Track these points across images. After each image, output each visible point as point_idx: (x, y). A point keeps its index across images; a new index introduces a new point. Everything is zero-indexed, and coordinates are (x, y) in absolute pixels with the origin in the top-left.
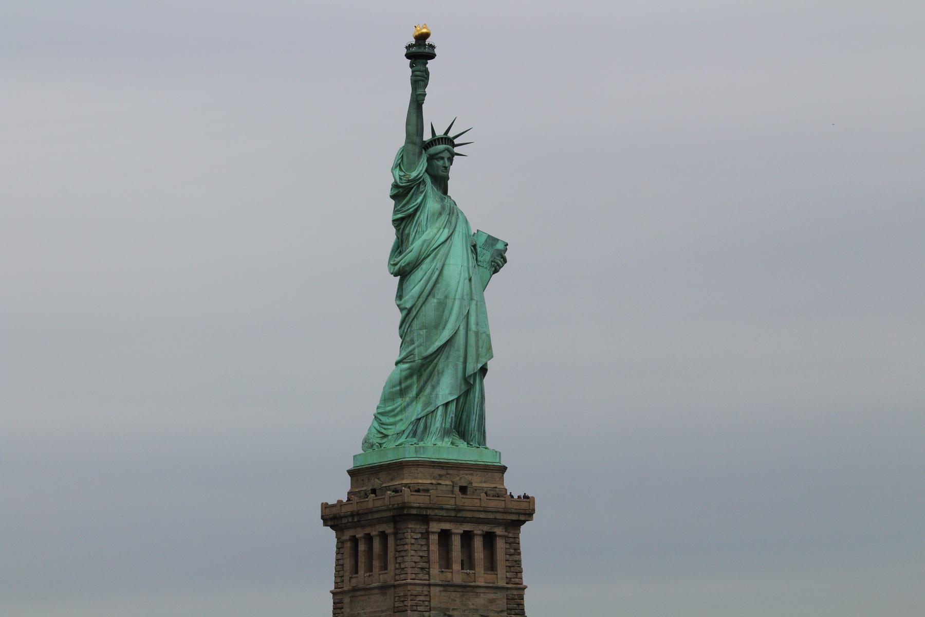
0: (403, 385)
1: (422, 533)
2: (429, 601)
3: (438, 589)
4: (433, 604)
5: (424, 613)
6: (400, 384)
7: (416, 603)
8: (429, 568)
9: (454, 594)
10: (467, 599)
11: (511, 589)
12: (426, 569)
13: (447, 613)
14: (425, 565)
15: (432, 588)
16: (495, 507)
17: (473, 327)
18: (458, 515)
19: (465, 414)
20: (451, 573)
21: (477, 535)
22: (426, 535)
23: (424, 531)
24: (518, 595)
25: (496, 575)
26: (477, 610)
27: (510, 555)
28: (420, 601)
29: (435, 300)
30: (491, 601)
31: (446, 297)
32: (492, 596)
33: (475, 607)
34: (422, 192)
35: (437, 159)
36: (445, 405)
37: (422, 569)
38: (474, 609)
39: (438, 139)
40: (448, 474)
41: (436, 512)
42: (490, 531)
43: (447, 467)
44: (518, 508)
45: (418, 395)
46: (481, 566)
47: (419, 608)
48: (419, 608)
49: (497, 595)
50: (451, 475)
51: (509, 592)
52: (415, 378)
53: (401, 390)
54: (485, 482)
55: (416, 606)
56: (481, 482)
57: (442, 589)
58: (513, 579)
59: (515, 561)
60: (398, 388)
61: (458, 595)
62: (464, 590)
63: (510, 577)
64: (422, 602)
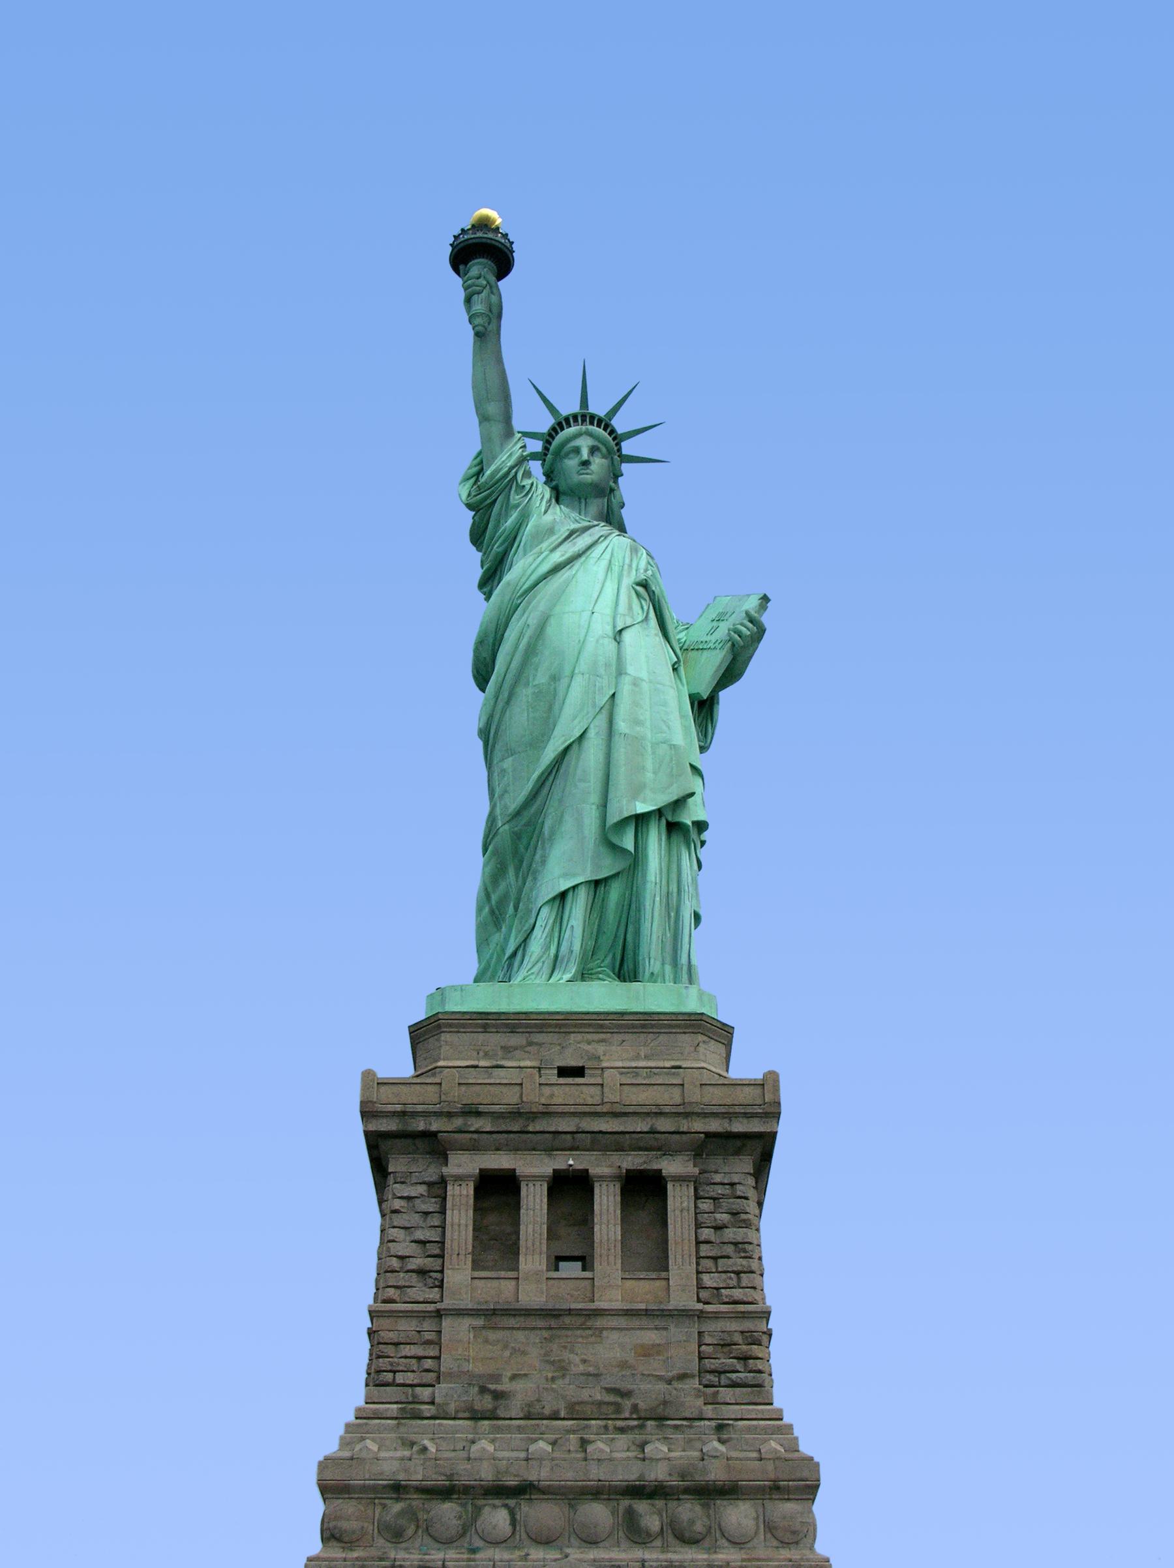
0: (494, 898)
1: (430, 1184)
2: (438, 1358)
3: (467, 1322)
4: (447, 1363)
5: (418, 1389)
6: (488, 896)
7: (391, 1364)
8: (442, 1272)
9: (520, 1336)
10: (565, 1347)
11: (717, 1316)
12: (432, 1274)
13: (492, 1387)
14: (434, 1264)
15: (446, 1323)
16: (651, 1102)
17: (622, 725)
18: (530, 1129)
19: (631, 929)
20: (513, 1283)
21: (602, 1178)
22: (439, 1188)
23: (434, 1178)
24: (742, 1332)
25: (664, 1283)
26: (597, 1375)
27: (718, 1228)
28: (406, 1357)
29: (530, 691)
30: (647, 1352)
31: (555, 678)
32: (651, 1337)
33: (591, 1369)
34: (517, 506)
35: (567, 455)
36: (557, 902)
37: (422, 1272)
38: (589, 1374)
39: (567, 419)
40: (530, 1044)
41: (458, 1122)
42: (642, 1168)
43: (527, 1026)
44: (729, 1101)
45: (516, 908)
46: (612, 1258)
47: (400, 1378)
48: (400, 1378)
49: (664, 1333)
50: (540, 1045)
51: (710, 1326)
52: (511, 872)
53: (492, 912)
54: (647, 1057)
55: (395, 1372)
56: (637, 1057)
57: (480, 1322)
58: (723, 1291)
59: (736, 1244)
60: (487, 910)
61: (535, 1337)
62: (553, 1323)
63: (715, 1285)
64: (414, 1361)
